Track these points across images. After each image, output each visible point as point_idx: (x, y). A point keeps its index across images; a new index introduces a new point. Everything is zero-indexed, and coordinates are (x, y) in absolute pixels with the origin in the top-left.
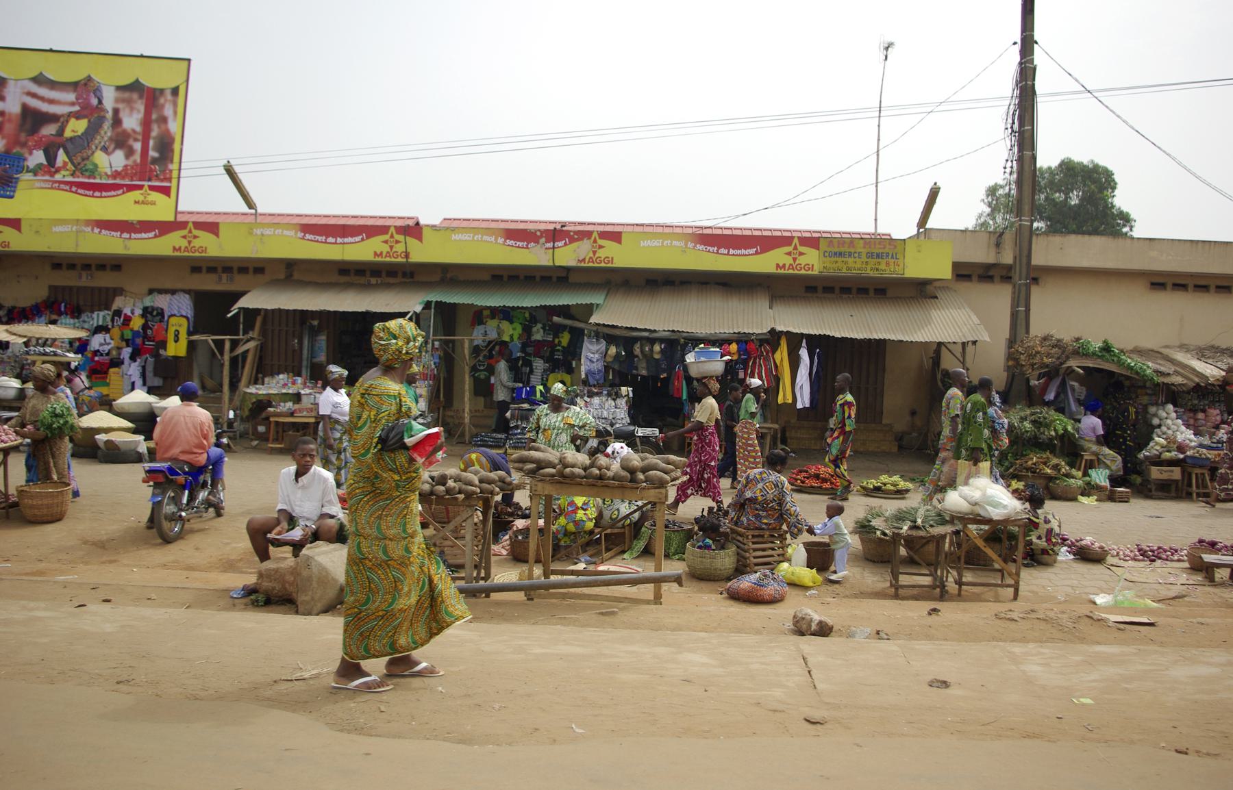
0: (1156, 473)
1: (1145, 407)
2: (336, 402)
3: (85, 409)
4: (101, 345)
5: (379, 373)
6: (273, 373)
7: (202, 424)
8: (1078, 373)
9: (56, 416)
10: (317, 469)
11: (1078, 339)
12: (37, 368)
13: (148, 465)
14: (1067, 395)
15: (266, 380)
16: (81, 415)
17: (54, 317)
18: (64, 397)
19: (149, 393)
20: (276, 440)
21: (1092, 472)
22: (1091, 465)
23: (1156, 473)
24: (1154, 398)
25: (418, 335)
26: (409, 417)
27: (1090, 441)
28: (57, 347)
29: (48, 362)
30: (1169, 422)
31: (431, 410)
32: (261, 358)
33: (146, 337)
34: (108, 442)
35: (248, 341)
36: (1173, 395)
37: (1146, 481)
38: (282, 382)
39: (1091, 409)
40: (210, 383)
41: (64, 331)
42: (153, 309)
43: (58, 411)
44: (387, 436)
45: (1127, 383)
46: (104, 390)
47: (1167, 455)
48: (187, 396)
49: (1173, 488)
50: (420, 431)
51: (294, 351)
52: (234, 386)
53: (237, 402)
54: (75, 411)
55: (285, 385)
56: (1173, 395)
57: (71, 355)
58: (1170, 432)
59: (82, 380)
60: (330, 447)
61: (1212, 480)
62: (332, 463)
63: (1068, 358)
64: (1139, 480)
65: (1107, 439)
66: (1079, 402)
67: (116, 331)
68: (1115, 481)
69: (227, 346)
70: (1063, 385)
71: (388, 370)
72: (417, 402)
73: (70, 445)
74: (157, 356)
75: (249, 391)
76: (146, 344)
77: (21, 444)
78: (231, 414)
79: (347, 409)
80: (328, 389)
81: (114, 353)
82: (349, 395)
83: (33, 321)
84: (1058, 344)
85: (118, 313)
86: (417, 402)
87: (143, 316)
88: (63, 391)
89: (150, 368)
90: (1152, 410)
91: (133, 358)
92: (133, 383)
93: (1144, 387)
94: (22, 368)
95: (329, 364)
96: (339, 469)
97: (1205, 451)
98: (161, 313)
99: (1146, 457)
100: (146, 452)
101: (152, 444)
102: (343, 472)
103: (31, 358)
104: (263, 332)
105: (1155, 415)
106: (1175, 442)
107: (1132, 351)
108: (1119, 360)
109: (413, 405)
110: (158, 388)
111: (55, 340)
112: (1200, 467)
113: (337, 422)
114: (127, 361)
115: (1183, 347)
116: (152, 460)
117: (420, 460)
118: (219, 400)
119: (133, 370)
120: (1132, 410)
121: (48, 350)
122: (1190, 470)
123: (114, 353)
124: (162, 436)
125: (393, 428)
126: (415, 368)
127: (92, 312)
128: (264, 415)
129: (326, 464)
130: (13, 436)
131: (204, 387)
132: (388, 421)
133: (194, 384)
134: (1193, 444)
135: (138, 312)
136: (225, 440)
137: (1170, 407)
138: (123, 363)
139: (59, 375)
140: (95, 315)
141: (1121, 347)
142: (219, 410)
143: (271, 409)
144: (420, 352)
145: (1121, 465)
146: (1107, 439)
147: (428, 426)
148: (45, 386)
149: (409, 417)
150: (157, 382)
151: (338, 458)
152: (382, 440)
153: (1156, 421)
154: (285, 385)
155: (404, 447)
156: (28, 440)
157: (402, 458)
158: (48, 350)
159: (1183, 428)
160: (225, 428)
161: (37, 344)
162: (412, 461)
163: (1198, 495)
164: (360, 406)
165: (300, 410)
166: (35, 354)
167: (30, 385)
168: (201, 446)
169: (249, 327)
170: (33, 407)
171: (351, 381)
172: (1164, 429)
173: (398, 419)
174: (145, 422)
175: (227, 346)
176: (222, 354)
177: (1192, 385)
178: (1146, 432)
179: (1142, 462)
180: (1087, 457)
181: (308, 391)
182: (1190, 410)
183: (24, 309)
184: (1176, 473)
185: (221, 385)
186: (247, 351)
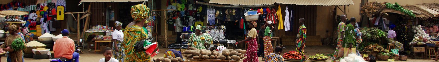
0: (416, 50)
1: (411, 26)
2: (118, 34)
3: (28, 40)
4: (33, 17)
5: (134, 24)
6: (95, 25)
7: (70, 44)
8: (386, 15)
9: (18, 43)
10: (113, 59)
11: (386, 3)
12: (10, 26)
13: (51, 60)
14: (383, 23)
15: (93, 27)
16: (26, 42)
17: (16, 8)
18: (20, 36)
19: (51, 33)
20: (97, 49)
21: (393, 50)
22: (392, 48)
23: (416, 50)
24: (414, 23)
25: (147, 10)
26: (145, 39)
27: (391, 39)
28: (17, 18)
29: (14, 24)
30: (420, 31)
31: (153, 36)
32: (91, 20)
33: (49, 14)
34: (37, 52)
35: (86, 14)
36: (421, 22)
37: (412, 53)
38: (99, 28)
39: (392, 28)
40: (73, 29)
41: (19, 13)
42: (51, 3)
43: (18, 41)
44: (138, 46)
45: (404, 18)
46: (35, 33)
47: (420, 43)
48: (65, 34)
49: (422, 54)
50: (149, 44)
51: (103, 17)
52: (81, 30)
53: (83, 36)
54: (24, 41)
55: (100, 29)
56: (421, 22)
57: (22, 21)
58: (420, 35)
59: (26, 30)
60: (117, 51)
61: (436, 52)
62: (118, 56)
63: (382, 10)
64: (410, 52)
65: (397, 39)
66: (387, 25)
67: (38, 12)
68: (401, 53)
69: (79, 16)
70: (381, 19)
71: (137, 22)
72: (148, 34)
73: (23, 53)
74: (53, 20)
75: (87, 32)
76: (49, 16)
77: (5, 54)
78: (81, 40)
79: (123, 37)
80: (116, 30)
81: (38, 20)
82: (123, 32)
83: (8, 9)
84: (379, 5)
85: (39, 5)
86: (148, 34)
87: (48, 6)
88: (20, 34)
89: (51, 25)
90: (414, 27)
91: (45, 21)
92: (45, 30)
93: (410, 19)
94: (5, 26)
95: (115, 21)
96: (121, 58)
97: (433, 41)
98: (54, 5)
99: (412, 44)
100: (51, 55)
101: (52, 52)
102: (122, 59)
103: (8, 23)
104: (91, 10)
105: (415, 29)
106: (422, 38)
107: (405, 6)
108: (401, 10)
109: (146, 35)
110: (54, 32)
111: (16, 16)
112: (432, 47)
113: (119, 42)
114: (42, 22)
115: (424, 4)
116: (53, 57)
117: (150, 54)
118: (76, 35)
119: (45, 26)
120: (406, 27)
121: (14, 19)
122: (428, 48)
123: (38, 20)
124: (56, 49)
125: (139, 43)
126: (147, 22)
127: (29, 5)
128: (93, 40)
129: (116, 57)
130: (2, 51)
131: (71, 31)
132: (137, 41)
133: (67, 30)
134: (429, 39)
135: (46, 5)
136: (79, 50)
137: (420, 26)
138: (41, 23)
139: (18, 28)
140: (30, 7)
141: (402, 5)
142: (77, 39)
143: (95, 38)
144: (148, 15)
145: (403, 47)
146: (397, 39)
147: (152, 42)
148: (13, 33)
149: (145, 39)
150: (54, 30)
151: (120, 55)
152: (135, 48)
153: (415, 31)
154: (100, 29)
155: (144, 50)
156: (8, 52)
157: (143, 54)
158: (14, 19)
159: (425, 33)
160: (79, 45)
161: (10, 18)
162: (147, 55)
163: (431, 57)
164: (127, 36)
165: (106, 38)
166: (9, 21)
167: (8, 32)
168: (70, 52)
169: (86, 9)
170: (9, 40)
171: (124, 27)
172: (418, 34)
173: (141, 40)
174: (50, 44)
175: (79, 16)
176: (77, 19)
177: (427, 18)
178: (412, 35)
179: (410, 46)
180: (391, 45)
181: (108, 31)
182: (427, 27)
183: (5, 5)
184: (423, 49)
185: (77, 30)
186: (86, 17)
